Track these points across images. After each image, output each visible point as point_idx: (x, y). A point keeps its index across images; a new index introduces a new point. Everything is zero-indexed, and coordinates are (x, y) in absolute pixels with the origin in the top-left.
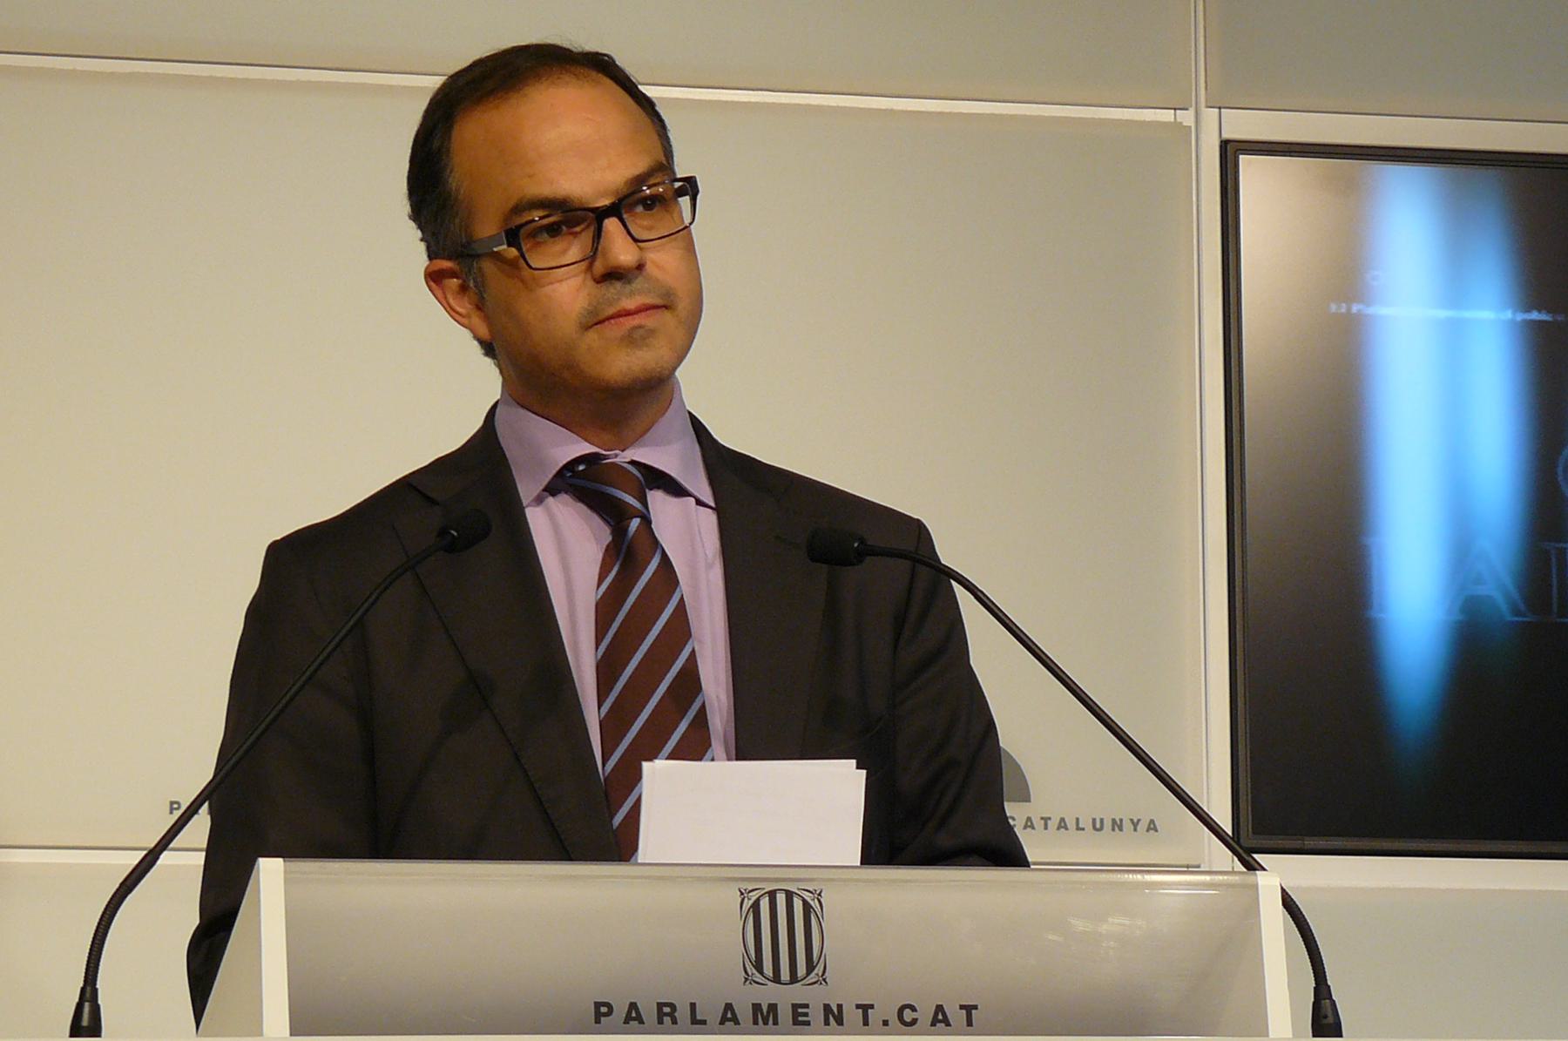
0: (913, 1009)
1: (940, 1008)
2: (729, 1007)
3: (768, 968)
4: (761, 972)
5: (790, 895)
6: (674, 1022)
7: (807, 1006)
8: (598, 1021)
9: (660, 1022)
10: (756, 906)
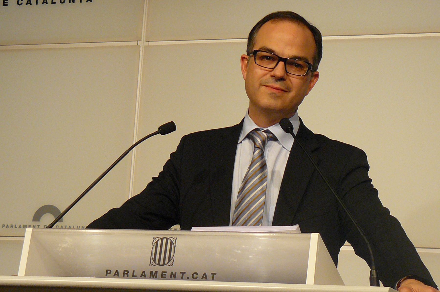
0: (197, 274)
1: (205, 274)
2: (144, 272)
4: (155, 262)
5: (167, 239)
6: (128, 276)
7: (166, 272)
8: (106, 275)
9: (124, 276)
10: (157, 243)
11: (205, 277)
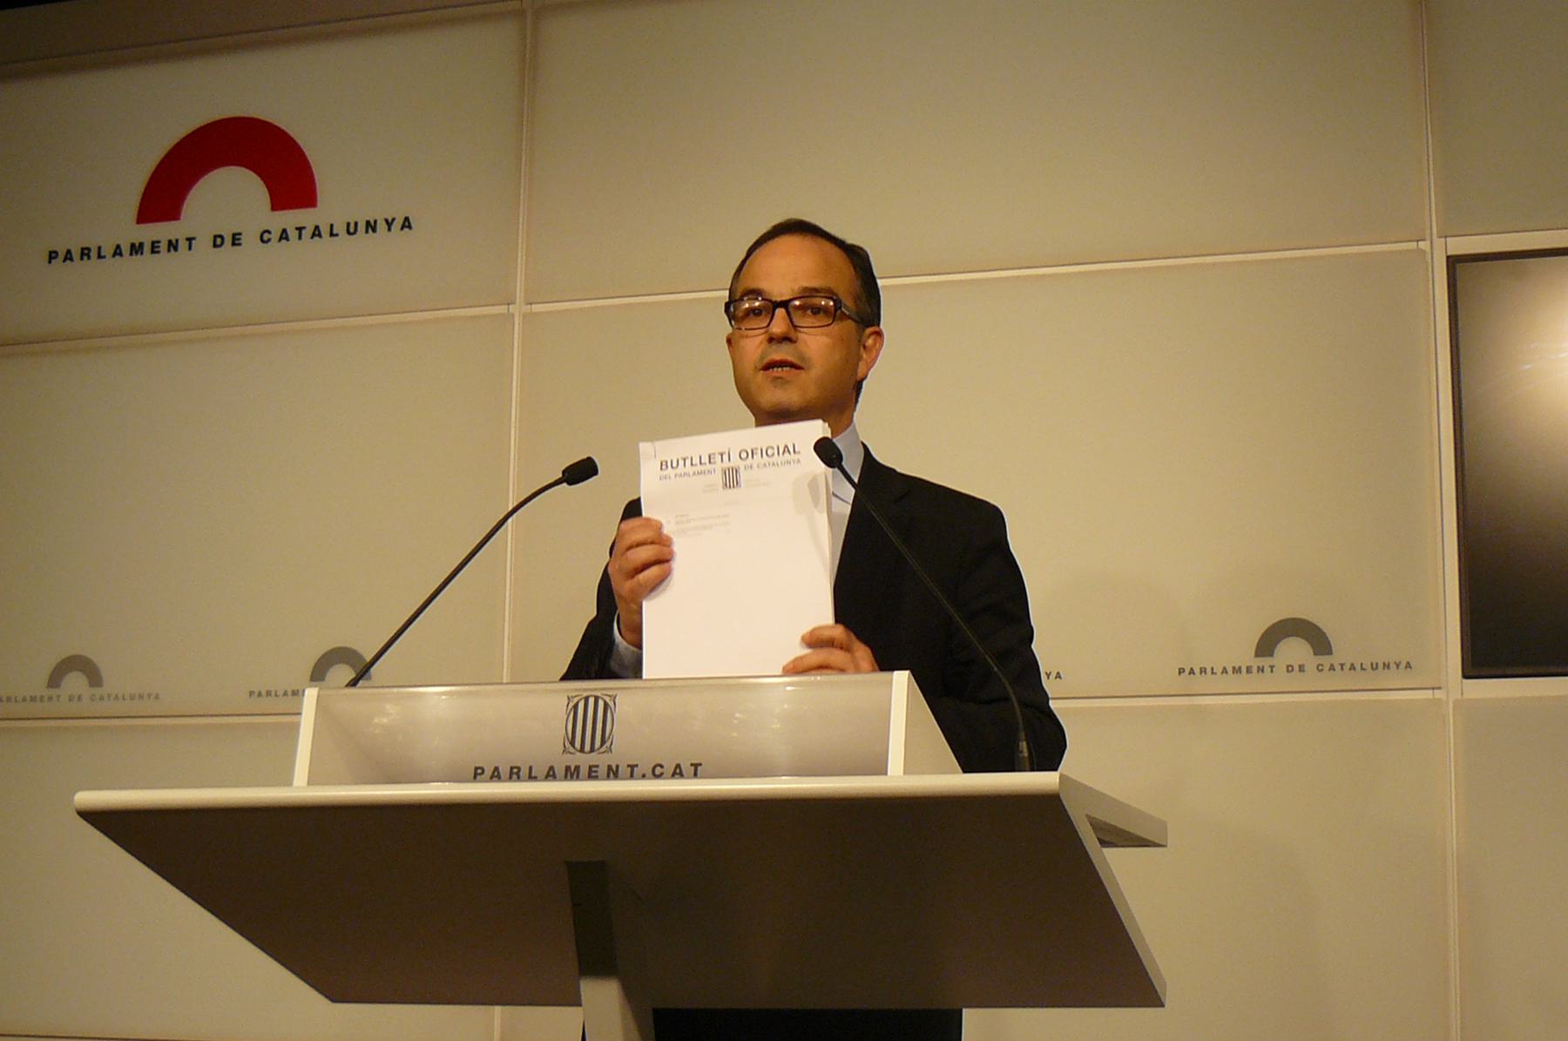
1: (678, 766)
2: (552, 768)
3: (578, 745)
5: (597, 699)
10: (576, 707)
11: (678, 773)
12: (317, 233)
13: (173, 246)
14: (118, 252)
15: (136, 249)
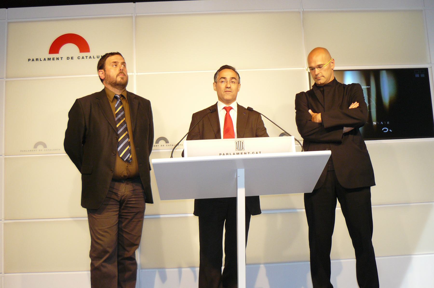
12: (90, 57)
13: (58, 59)
14: (45, 59)
15: (49, 59)
